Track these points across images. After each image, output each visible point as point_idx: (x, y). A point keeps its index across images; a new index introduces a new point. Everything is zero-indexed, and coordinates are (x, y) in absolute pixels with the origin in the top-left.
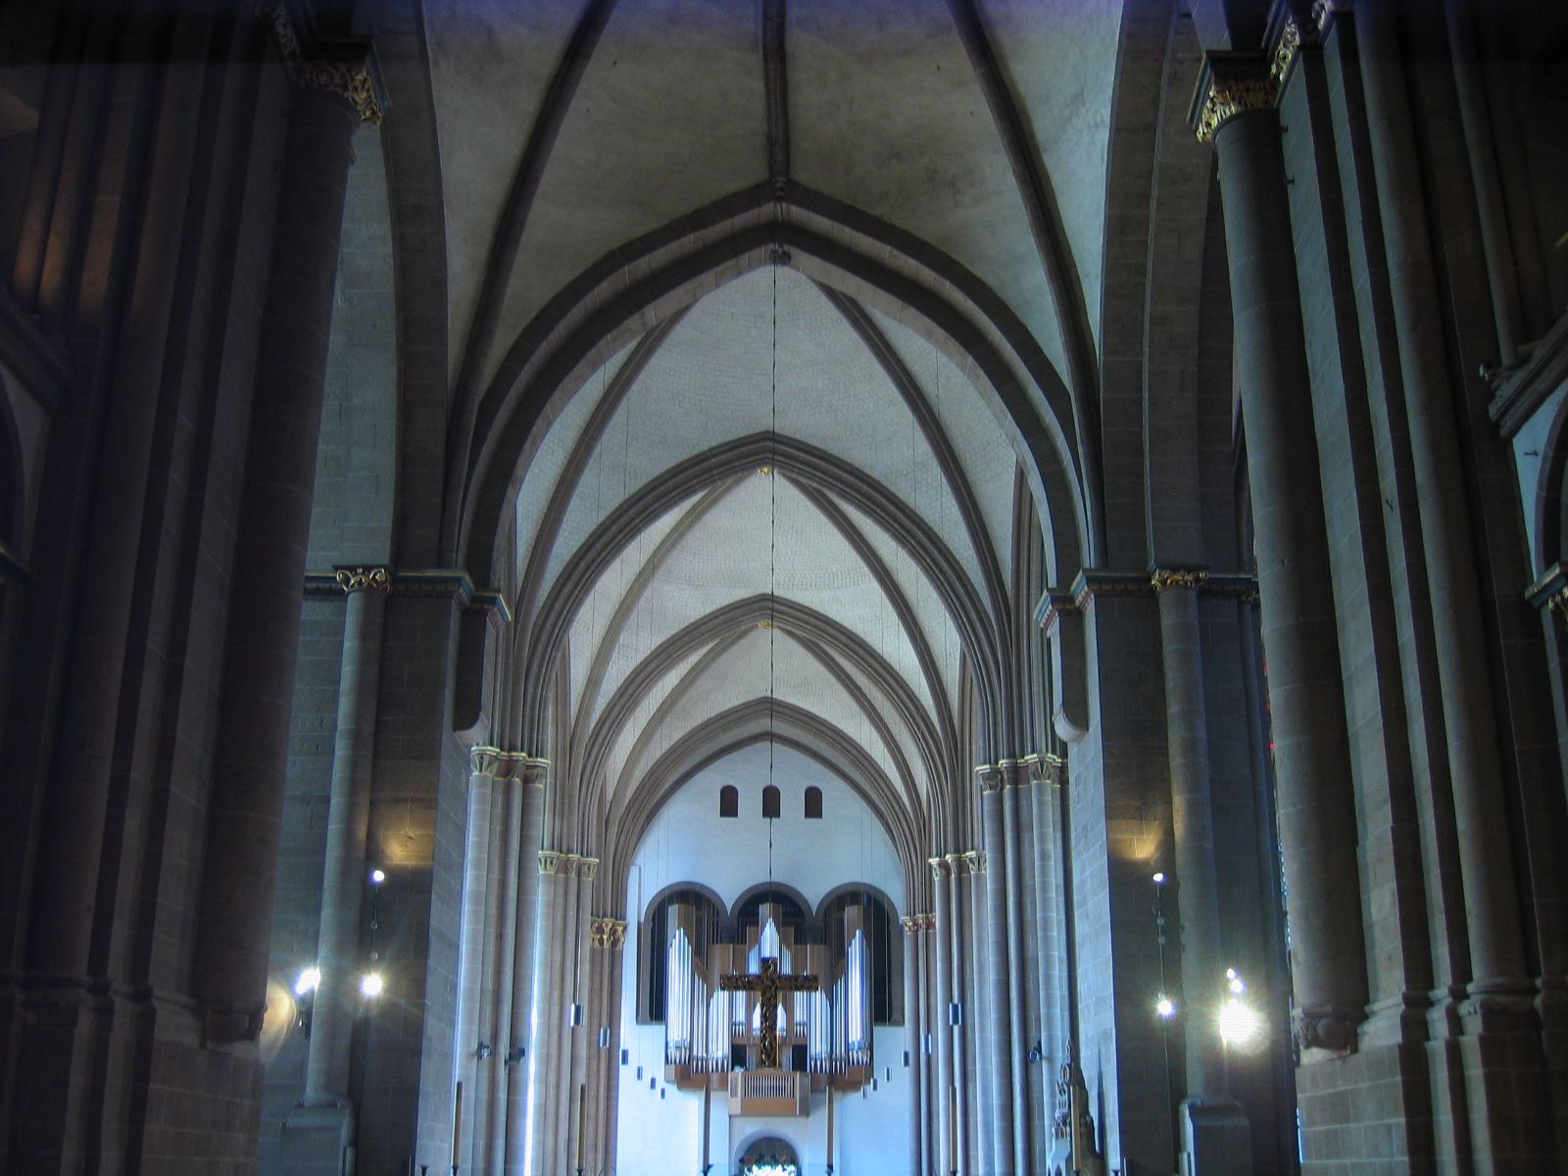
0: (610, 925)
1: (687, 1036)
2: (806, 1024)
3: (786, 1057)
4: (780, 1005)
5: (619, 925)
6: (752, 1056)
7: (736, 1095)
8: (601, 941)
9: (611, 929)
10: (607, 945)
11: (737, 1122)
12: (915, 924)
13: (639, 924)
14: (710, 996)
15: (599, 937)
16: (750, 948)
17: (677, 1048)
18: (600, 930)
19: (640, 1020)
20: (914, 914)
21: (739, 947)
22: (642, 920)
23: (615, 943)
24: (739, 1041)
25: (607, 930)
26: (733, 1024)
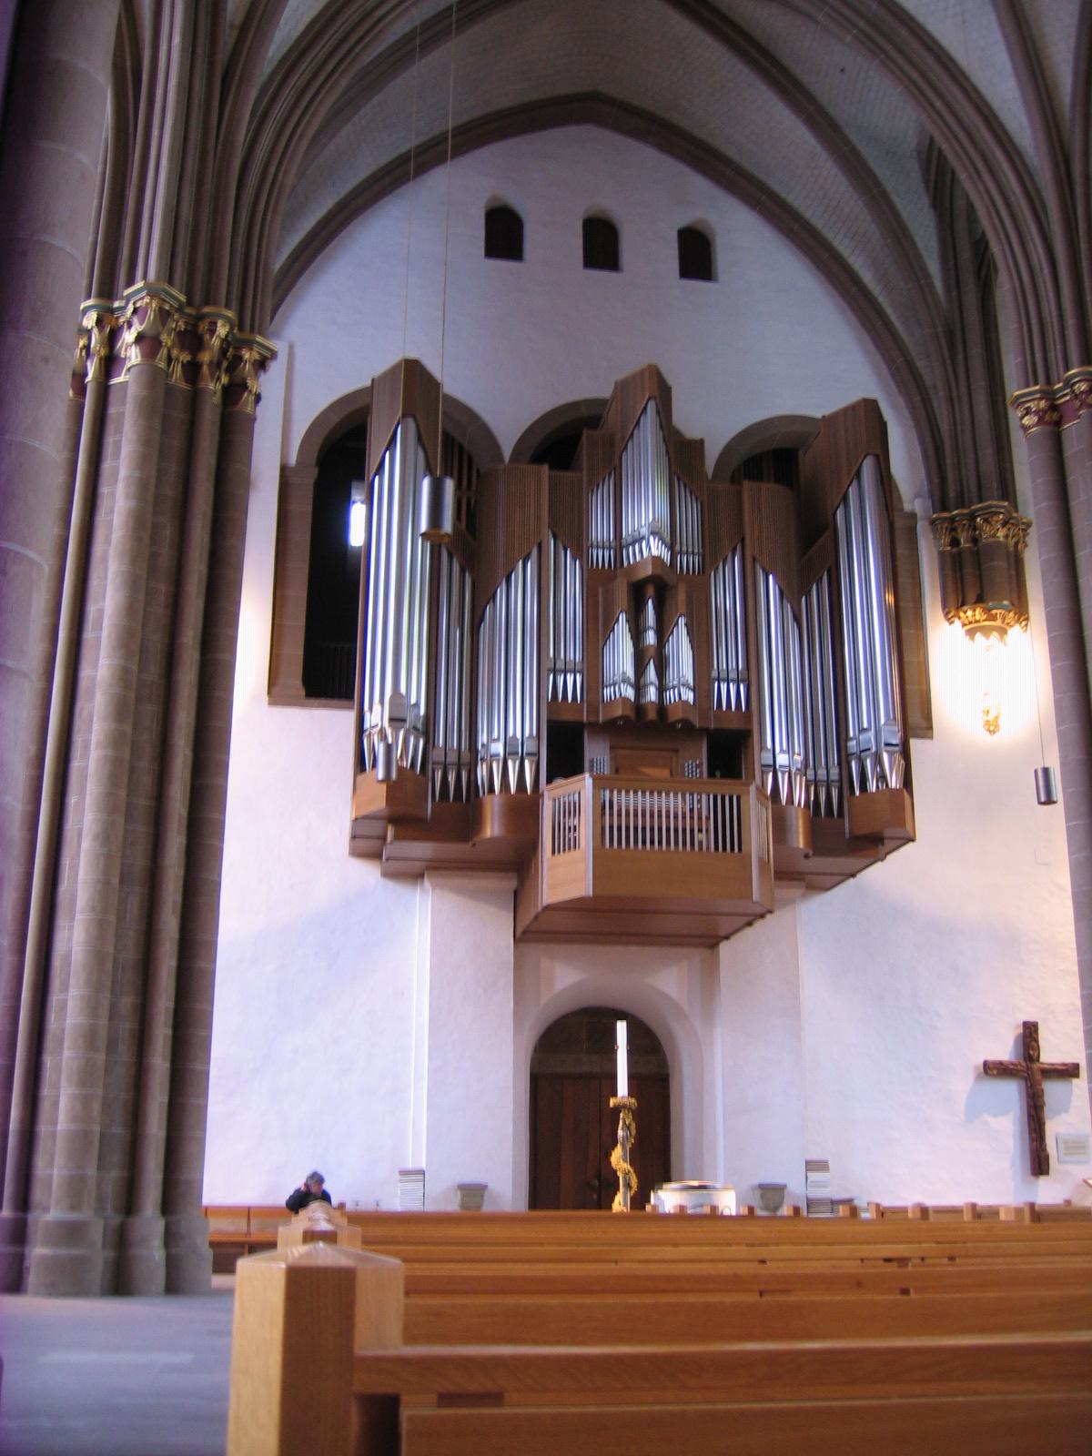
0: (222, 330)
1: (416, 693)
2: (750, 676)
3: (696, 760)
4: (682, 621)
5: (250, 344)
6: (596, 752)
7: (573, 845)
8: (192, 371)
9: (223, 351)
10: (213, 387)
11: (533, 950)
12: (1053, 408)
13: (284, 469)
14: (482, 599)
15: (185, 357)
16: (594, 485)
17: (396, 721)
18: (192, 339)
19: (276, 692)
20: (1049, 381)
21: (565, 475)
22: (293, 460)
23: (234, 391)
24: (567, 716)
25: (215, 342)
26: (547, 668)
